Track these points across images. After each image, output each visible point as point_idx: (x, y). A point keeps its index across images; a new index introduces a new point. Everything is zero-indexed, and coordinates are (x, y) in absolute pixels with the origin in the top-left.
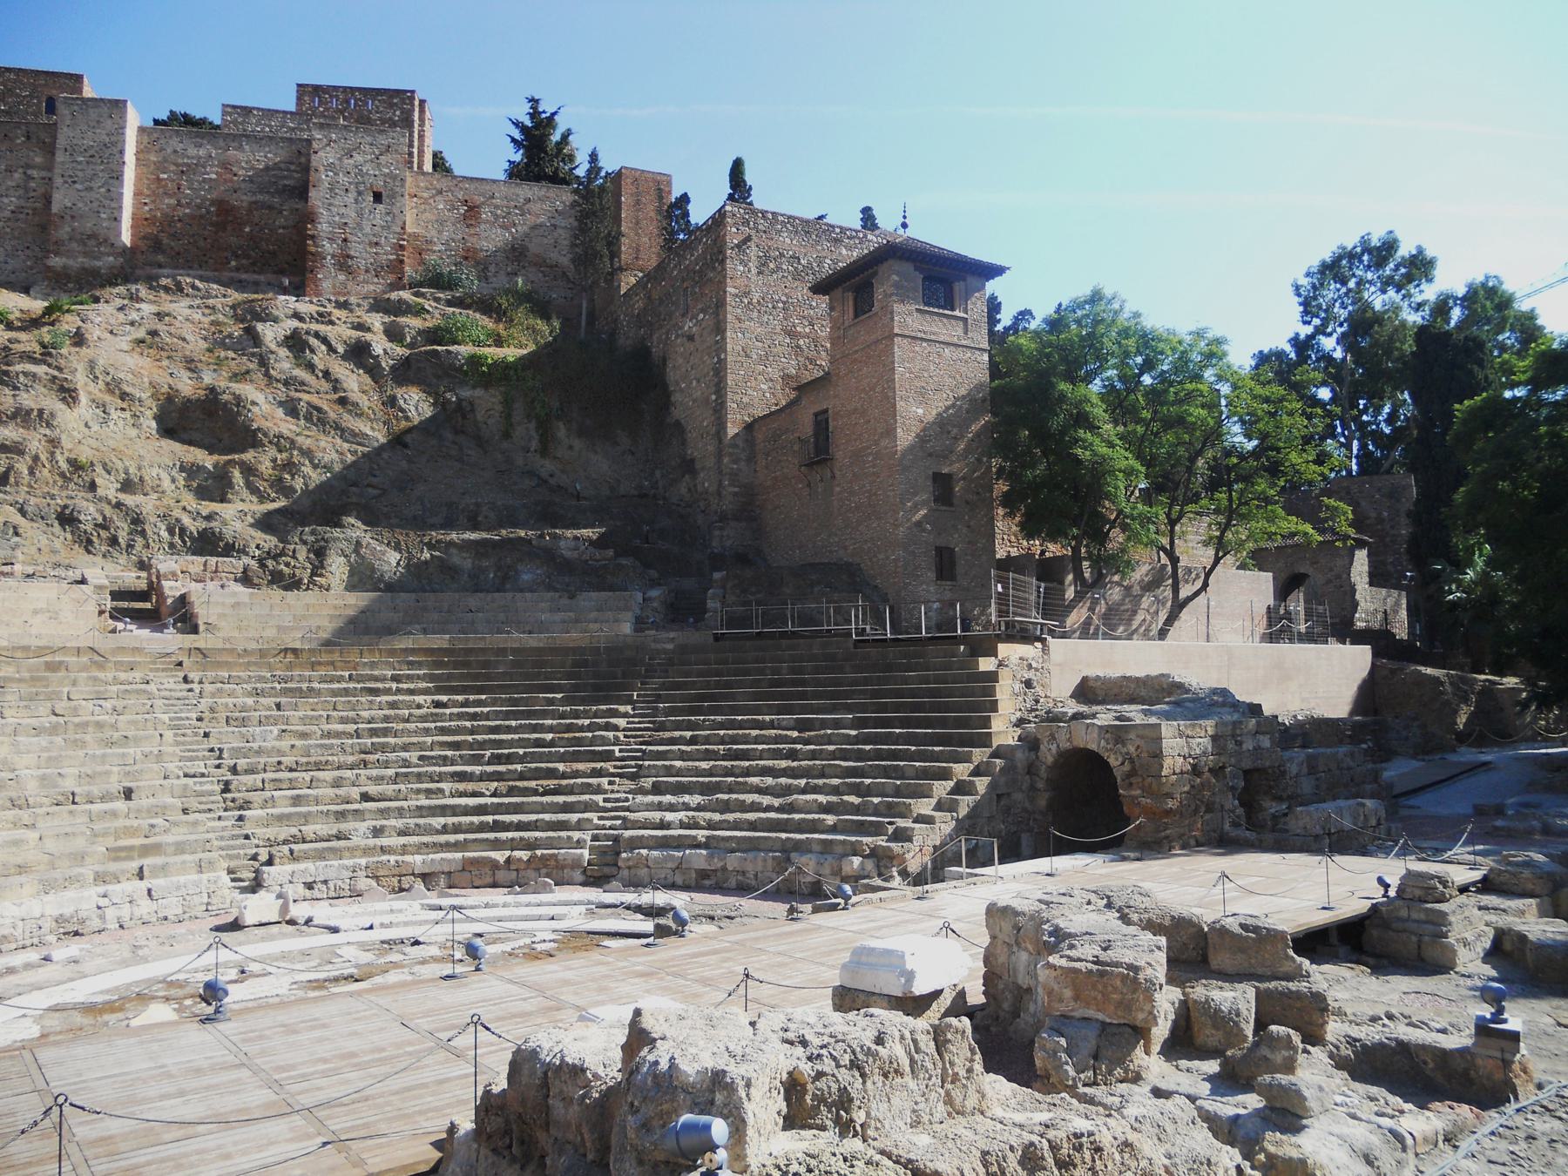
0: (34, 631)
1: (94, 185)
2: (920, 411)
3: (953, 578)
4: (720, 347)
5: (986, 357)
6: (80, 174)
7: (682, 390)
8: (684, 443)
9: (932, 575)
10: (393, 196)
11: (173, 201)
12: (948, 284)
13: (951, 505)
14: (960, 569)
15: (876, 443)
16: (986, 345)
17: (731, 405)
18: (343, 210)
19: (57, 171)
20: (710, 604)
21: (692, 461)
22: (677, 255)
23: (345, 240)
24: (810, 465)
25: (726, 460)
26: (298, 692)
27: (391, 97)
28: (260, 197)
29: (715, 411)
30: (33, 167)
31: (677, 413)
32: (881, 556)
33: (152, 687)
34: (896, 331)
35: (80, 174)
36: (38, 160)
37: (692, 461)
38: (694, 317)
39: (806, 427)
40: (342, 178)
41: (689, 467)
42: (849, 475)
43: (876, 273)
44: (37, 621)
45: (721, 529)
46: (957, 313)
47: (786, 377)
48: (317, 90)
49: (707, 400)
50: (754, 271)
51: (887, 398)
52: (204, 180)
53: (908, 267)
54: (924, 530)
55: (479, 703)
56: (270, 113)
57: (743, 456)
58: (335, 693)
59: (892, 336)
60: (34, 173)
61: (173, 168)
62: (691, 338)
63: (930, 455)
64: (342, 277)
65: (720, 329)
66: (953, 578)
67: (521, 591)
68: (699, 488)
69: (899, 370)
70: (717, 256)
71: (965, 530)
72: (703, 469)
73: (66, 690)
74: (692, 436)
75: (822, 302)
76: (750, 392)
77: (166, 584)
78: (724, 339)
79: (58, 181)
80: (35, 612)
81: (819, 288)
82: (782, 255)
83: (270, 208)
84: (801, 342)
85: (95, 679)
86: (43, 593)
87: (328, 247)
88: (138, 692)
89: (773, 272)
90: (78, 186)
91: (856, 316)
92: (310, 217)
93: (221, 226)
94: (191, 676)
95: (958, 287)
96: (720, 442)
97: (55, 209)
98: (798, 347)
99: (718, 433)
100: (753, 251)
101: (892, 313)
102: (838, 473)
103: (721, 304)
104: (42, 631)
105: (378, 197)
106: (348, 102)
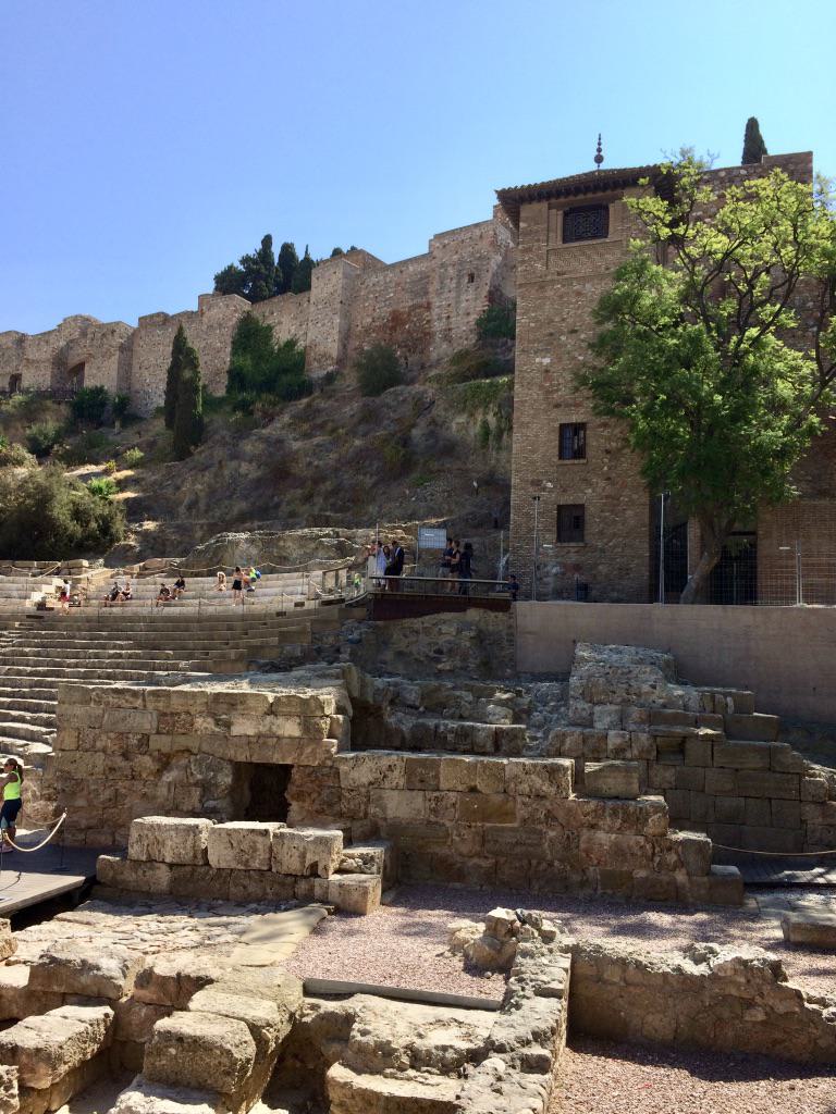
2: (547, 361)
10: (479, 276)
11: (369, 320)
12: (601, 210)
23: (449, 317)
53: (544, 205)
54: (544, 489)
61: (372, 296)
63: (557, 406)
71: (602, 484)
87: (438, 326)
90: (319, 325)
105: (472, 278)
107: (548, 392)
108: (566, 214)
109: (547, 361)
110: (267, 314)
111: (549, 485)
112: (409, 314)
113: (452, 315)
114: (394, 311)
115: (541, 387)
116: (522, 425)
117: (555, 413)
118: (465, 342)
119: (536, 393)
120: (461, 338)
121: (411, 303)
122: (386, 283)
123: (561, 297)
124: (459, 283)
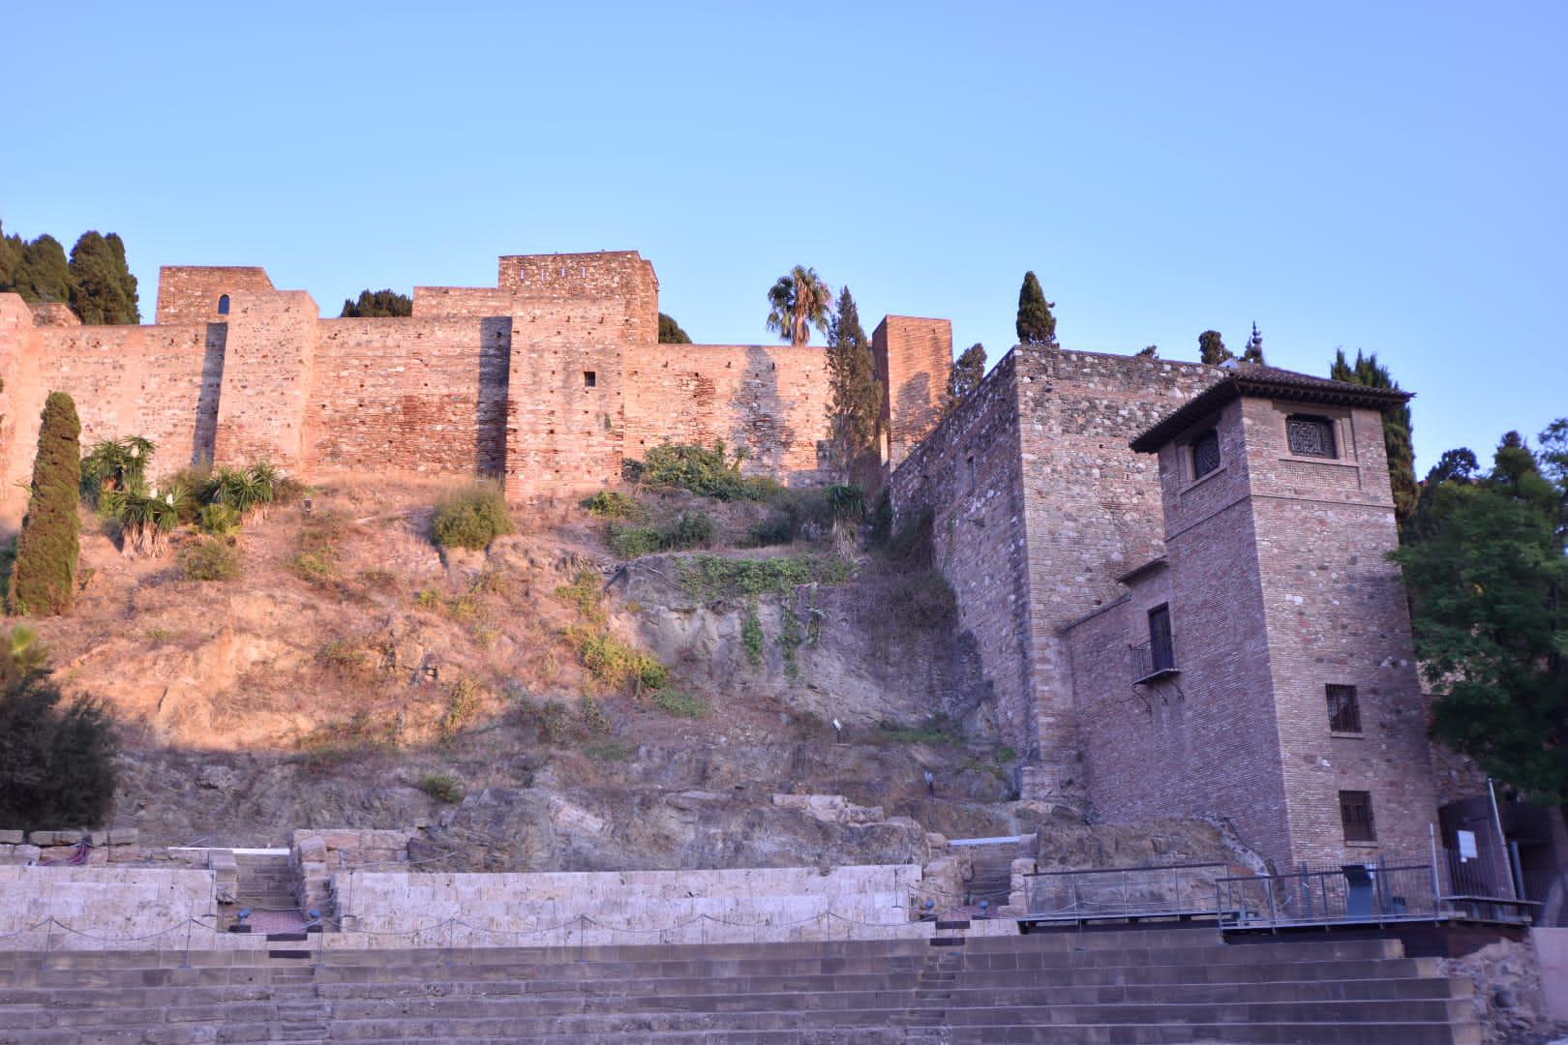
0: (137, 932)
1: (267, 389)
2: (1299, 600)
3: (1370, 836)
4: (1017, 532)
5: (1391, 518)
6: (251, 378)
7: (972, 592)
8: (977, 660)
9: (1338, 832)
11: (354, 402)
13: (1358, 730)
14: (1381, 822)
15: (1239, 646)
16: (1390, 502)
17: (1034, 606)
18: (549, 396)
19: (225, 377)
20: (1017, 880)
21: (990, 684)
22: (959, 418)
24: (1152, 683)
26: (458, 1009)
28: (454, 390)
29: (1016, 615)
31: (967, 622)
32: (1258, 807)
33: (273, 1003)
34: (1254, 491)
35: (251, 378)
37: (990, 684)
38: (984, 494)
39: (1139, 630)
40: (552, 361)
41: (986, 692)
42: (1204, 695)
43: (1219, 418)
44: (141, 919)
45: (1032, 774)
46: (1342, 461)
47: (1109, 565)
48: (522, 260)
49: (1004, 600)
50: (1057, 430)
51: (1248, 583)
52: (389, 376)
53: (1264, 407)
54: (1320, 768)
55: (694, 1024)
56: (469, 292)
57: (1057, 674)
58: (504, 1010)
59: (1247, 500)
62: (980, 524)
63: (1320, 660)
64: (548, 476)
65: (1016, 507)
66: (1370, 836)
67: (760, 865)
68: (1001, 719)
69: (1263, 544)
70: (1007, 416)
71: (1384, 766)
72: (1004, 694)
73: (164, 1009)
74: (986, 651)
75: (1149, 462)
76: (1061, 587)
77: (308, 865)
78: (1022, 520)
79: (225, 387)
80: (142, 906)
81: (1141, 445)
82: (1093, 407)
84: (1128, 517)
85: (203, 994)
86: (151, 881)
88: (253, 1010)
89: (1082, 428)
90: (248, 391)
91: (1197, 476)
93: (409, 426)
94: (324, 988)
95: (1342, 426)
97: (220, 418)
98: (1125, 524)
99: (1021, 645)
100: (1054, 406)
101: (1245, 468)
102: (1188, 694)
103: (1016, 476)
104: (144, 932)
105: (590, 377)
106: (558, 272)
107: (1308, 641)
108: (1289, 418)
109: (1299, 600)
110: (82, 343)
111: (1325, 763)
112: (441, 409)
113: (557, 429)
114: (409, 398)
115: (1298, 633)
116: (1284, 680)
117: (1318, 670)
118: (587, 477)
119: (1292, 640)
120: (577, 468)
121: (445, 391)
122: (385, 347)
123: (1304, 520)
124: (566, 380)
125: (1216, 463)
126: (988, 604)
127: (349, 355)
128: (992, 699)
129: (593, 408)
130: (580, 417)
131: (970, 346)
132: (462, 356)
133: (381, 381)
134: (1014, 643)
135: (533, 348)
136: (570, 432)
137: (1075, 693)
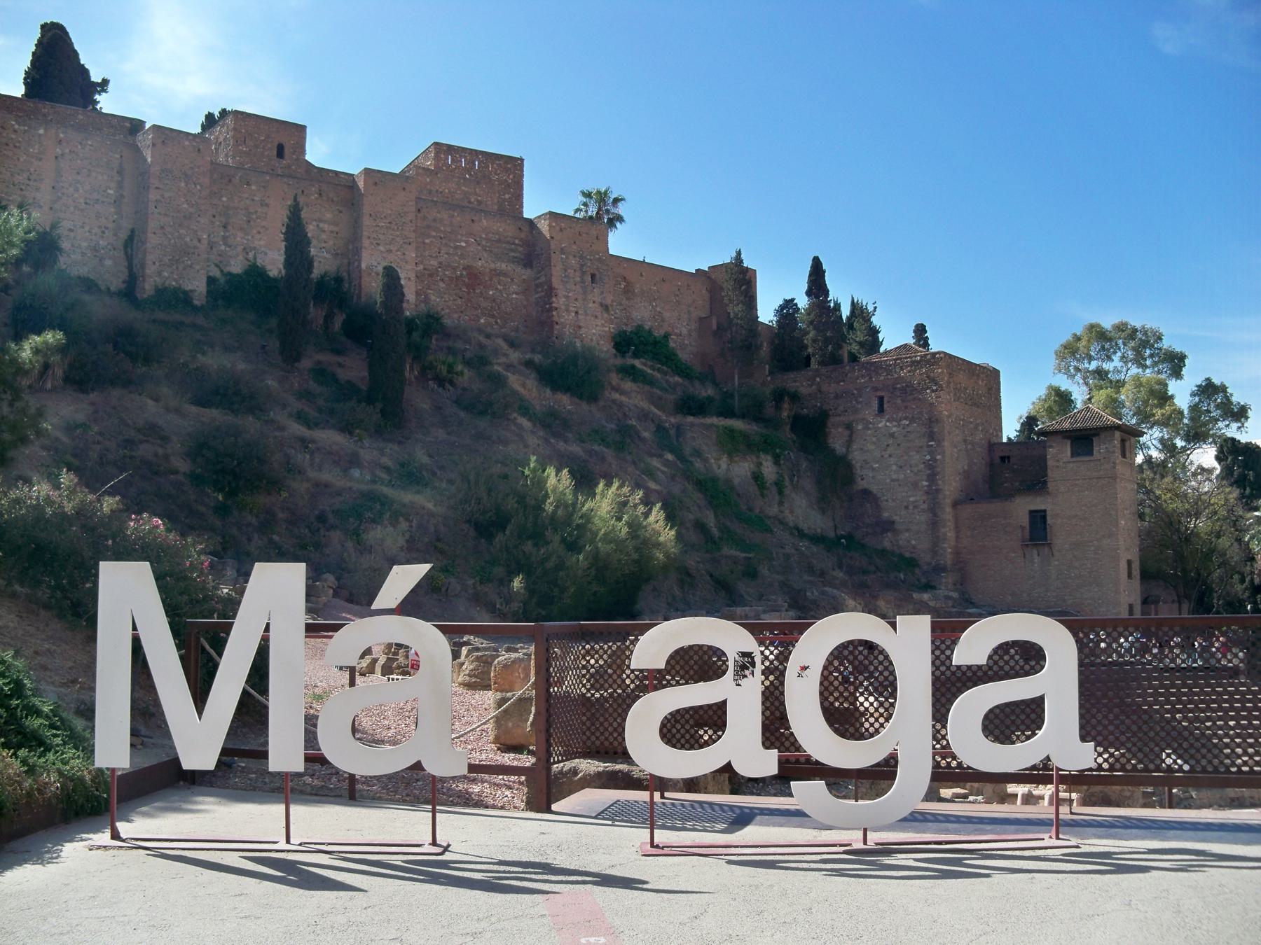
6: (382, 237)
7: (873, 469)
8: (878, 506)
18: (574, 288)
21: (893, 522)
25: (943, 530)
27: (506, 163)
30: (324, 222)
36: (329, 216)
39: (1025, 520)
41: (888, 526)
43: (1097, 435)
49: (915, 485)
52: (456, 248)
60: (326, 227)
62: (892, 435)
72: (907, 530)
83: (505, 275)
90: (381, 248)
91: (1072, 456)
92: (550, 291)
96: (935, 515)
125: (1090, 453)
126: (893, 480)
127: (429, 227)
128: (896, 532)
129: (598, 300)
130: (591, 305)
131: (788, 298)
132: (499, 241)
133: (451, 251)
134: (925, 506)
135: (562, 251)
136: (586, 314)
137: (957, 537)
